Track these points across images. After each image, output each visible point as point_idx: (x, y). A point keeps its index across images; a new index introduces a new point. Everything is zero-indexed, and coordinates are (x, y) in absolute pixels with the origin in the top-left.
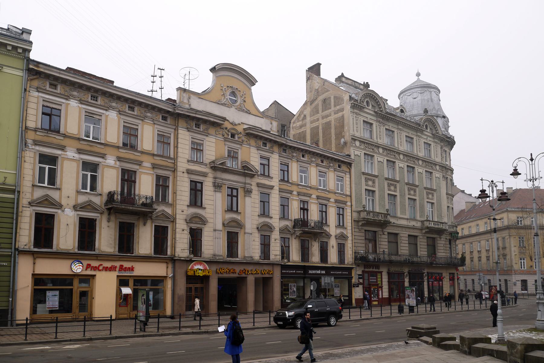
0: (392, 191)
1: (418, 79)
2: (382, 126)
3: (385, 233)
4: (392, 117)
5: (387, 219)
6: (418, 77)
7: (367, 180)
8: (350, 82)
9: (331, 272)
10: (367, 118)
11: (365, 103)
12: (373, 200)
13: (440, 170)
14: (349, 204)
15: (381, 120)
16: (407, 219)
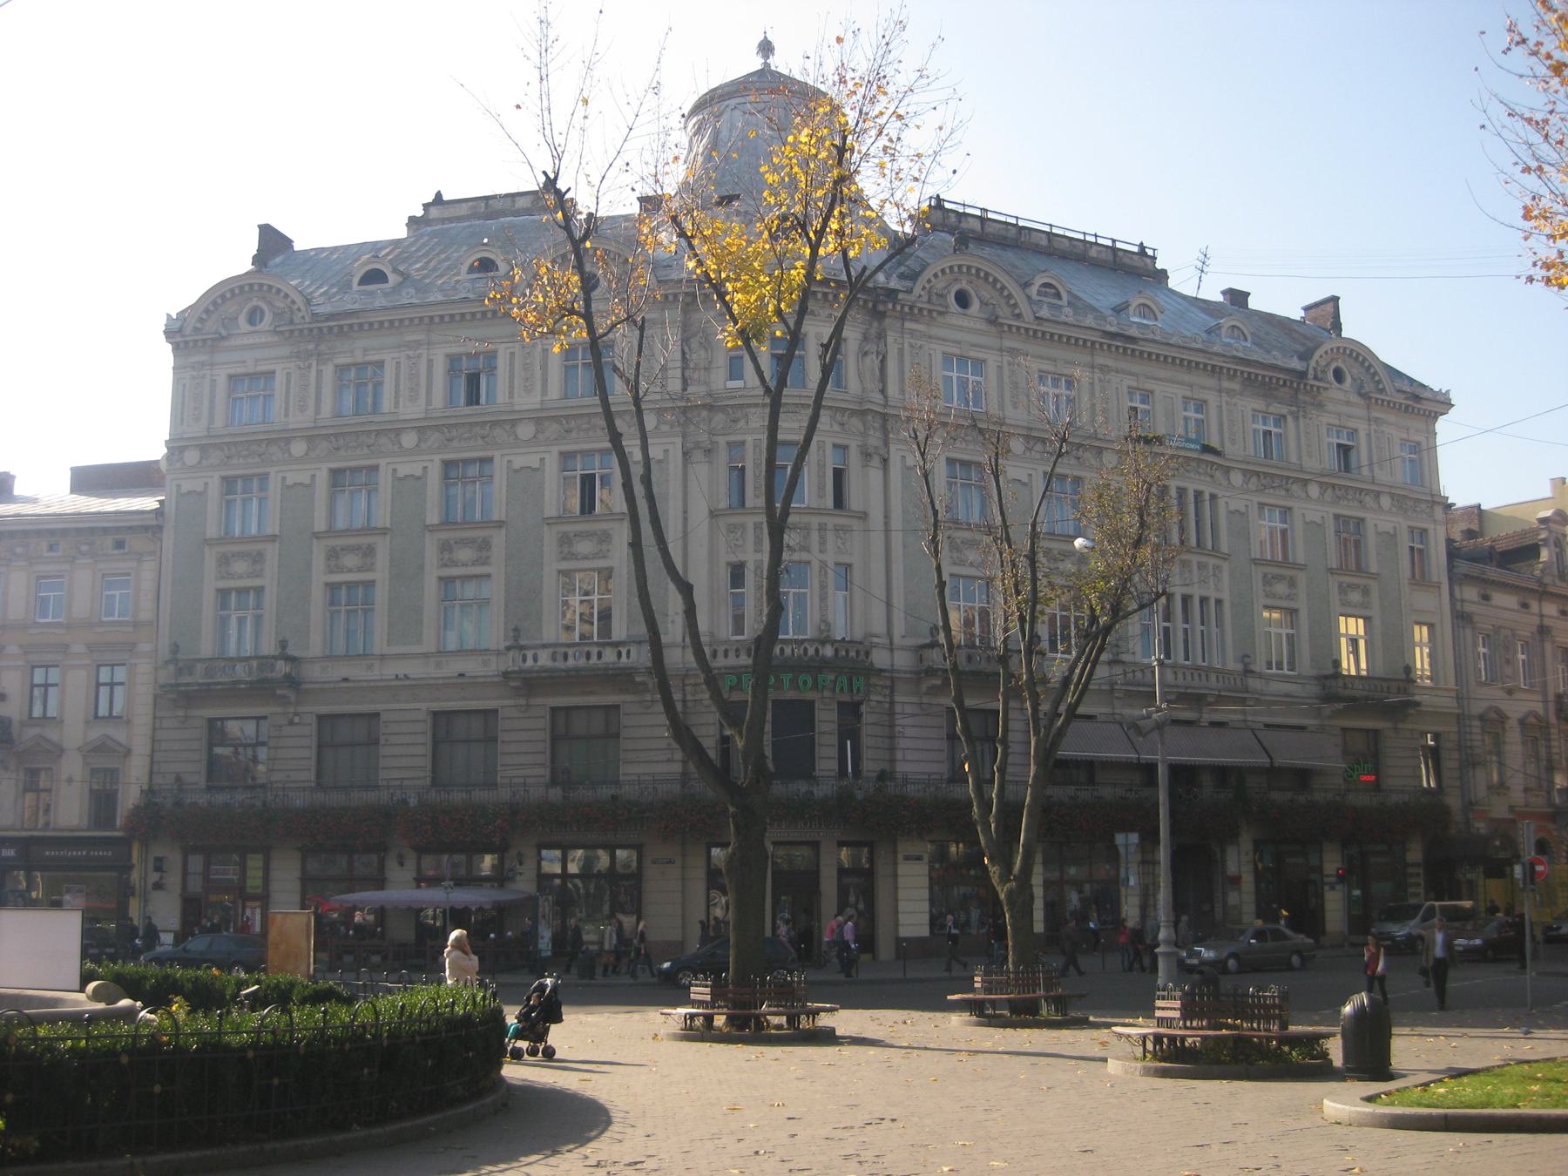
0: (350, 571)
1: (767, 65)
2: (314, 363)
3: (297, 720)
4: (342, 323)
5: (273, 674)
6: (766, 57)
7: (224, 560)
8: (463, 210)
9: (47, 853)
10: (244, 362)
11: (242, 320)
12: (258, 620)
13: (665, 428)
14: (145, 647)
15: (311, 346)
16: (426, 655)
